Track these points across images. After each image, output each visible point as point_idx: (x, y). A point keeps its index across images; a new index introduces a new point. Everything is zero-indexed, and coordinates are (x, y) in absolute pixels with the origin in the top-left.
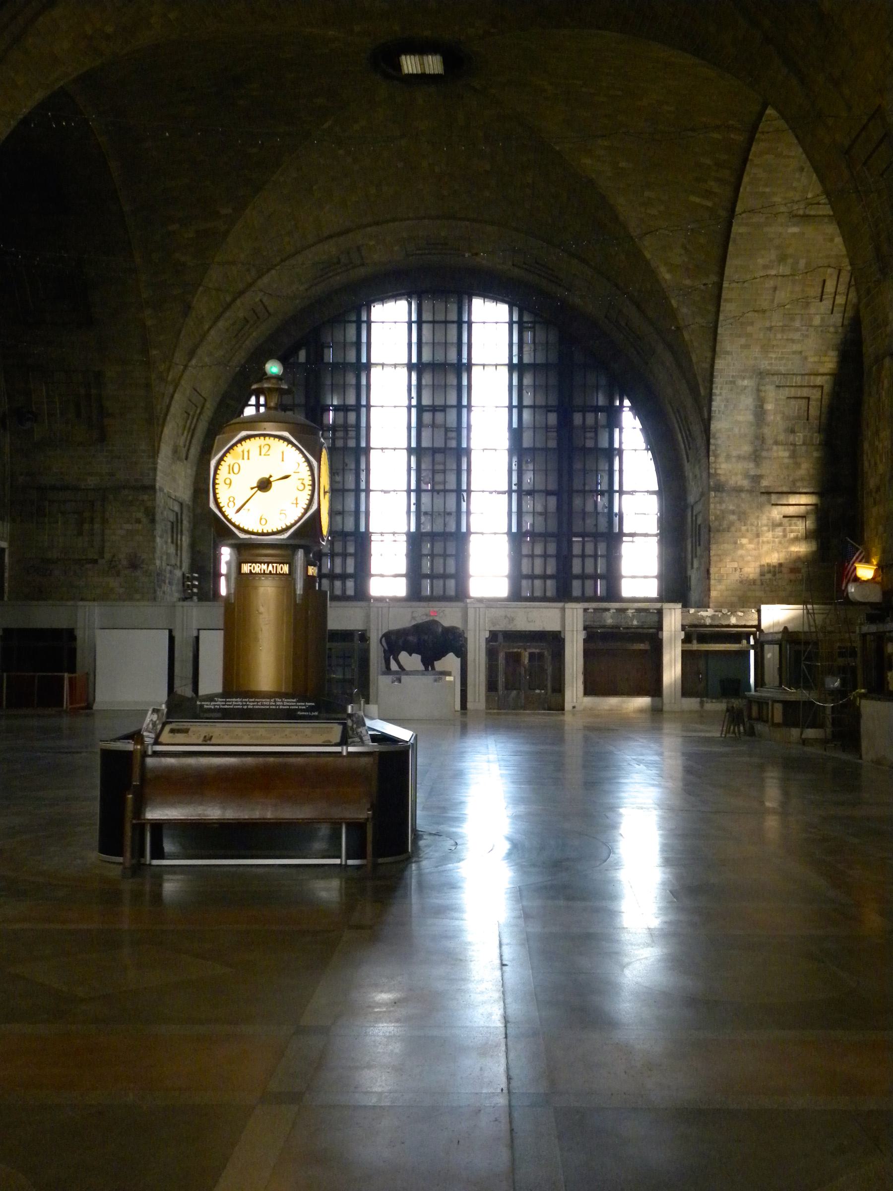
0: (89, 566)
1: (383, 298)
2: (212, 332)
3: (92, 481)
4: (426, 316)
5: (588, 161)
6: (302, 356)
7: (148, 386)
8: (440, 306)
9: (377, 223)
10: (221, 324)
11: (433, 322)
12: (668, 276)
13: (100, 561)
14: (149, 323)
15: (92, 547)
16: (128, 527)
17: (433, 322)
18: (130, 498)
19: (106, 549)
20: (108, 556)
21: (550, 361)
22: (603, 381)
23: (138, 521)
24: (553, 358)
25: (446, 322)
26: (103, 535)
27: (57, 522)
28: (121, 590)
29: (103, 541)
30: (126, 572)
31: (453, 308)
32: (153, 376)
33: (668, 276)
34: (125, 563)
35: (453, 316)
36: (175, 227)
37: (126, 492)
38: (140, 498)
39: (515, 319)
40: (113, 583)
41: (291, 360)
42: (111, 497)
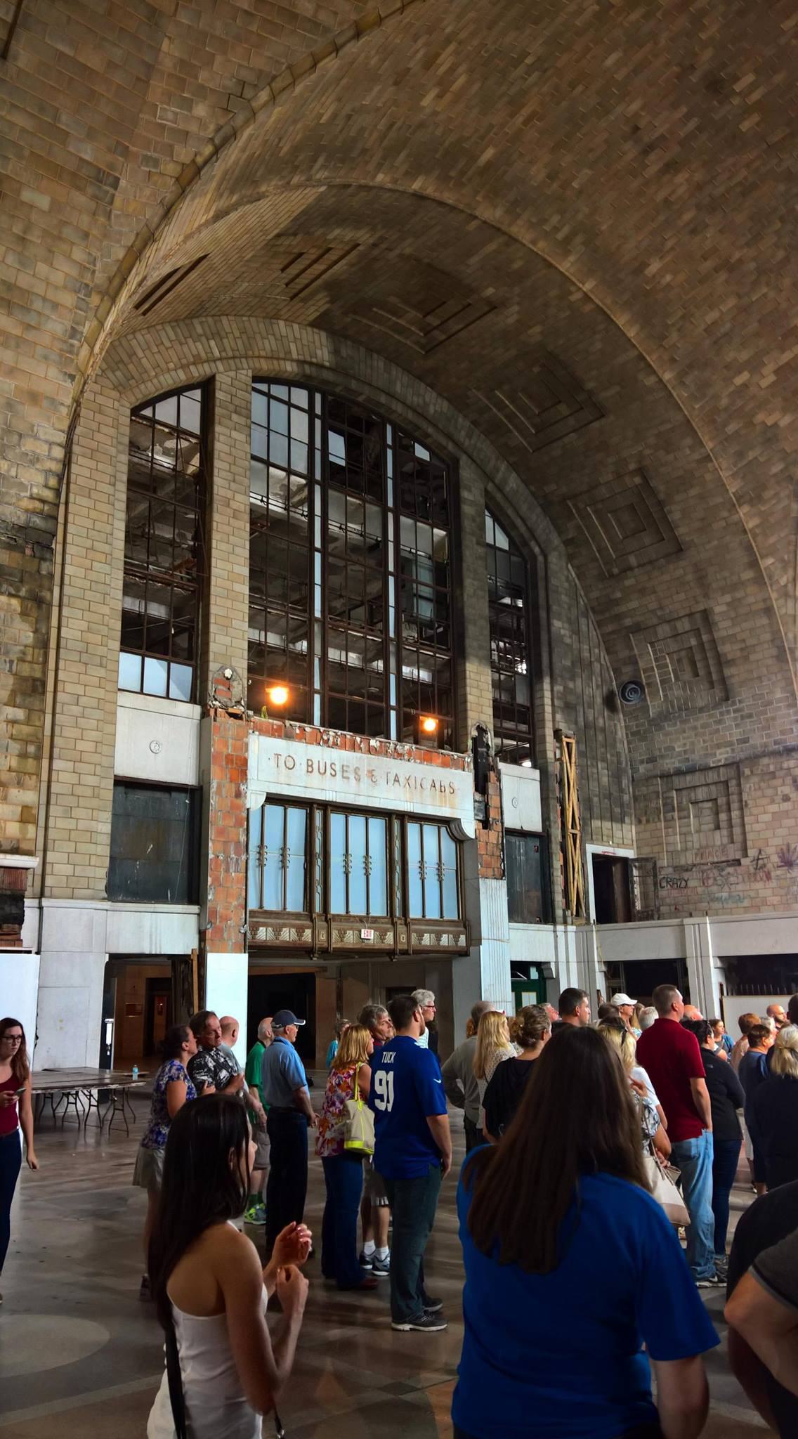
0: (731, 870)
3: (722, 756)
7: (769, 611)
13: (743, 861)
14: (750, 525)
15: (732, 842)
16: (773, 808)
18: (772, 768)
19: (749, 844)
20: (752, 853)
23: (786, 798)
26: (743, 825)
27: (689, 817)
28: (776, 900)
29: (744, 833)
30: (779, 872)
32: (774, 595)
34: (775, 859)
37: (765, 761)
38: (785, 765)
40: (763, 889)
42: (747, 772)
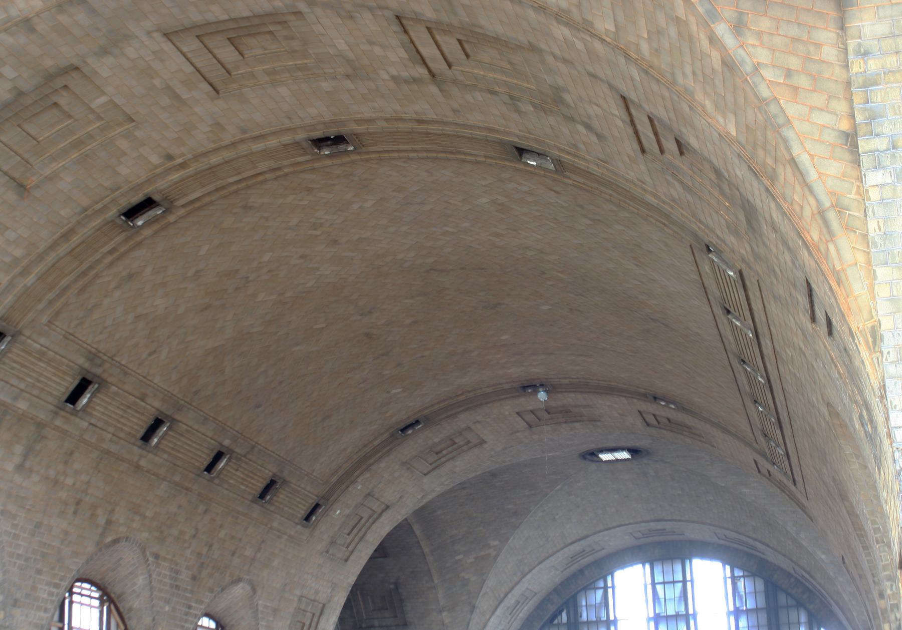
1: (623, 565)
2: (492, 619)
4: (659, 578)
5: (745, 490)
6: (564, 615)
8: (668, 567)
9: (607, 530)
10: (498, 612)
11: (664, 583)
12: (823, 557)
17: (664, 583)
21: (759, 606)
22: (803, 618)
24: (762, 603)
25: (674, 582)
31: (678, 567)
33: (823, 557)
35: (679, 577)
36: (461, 557)
39: (728, 574)
41: (556, 622)
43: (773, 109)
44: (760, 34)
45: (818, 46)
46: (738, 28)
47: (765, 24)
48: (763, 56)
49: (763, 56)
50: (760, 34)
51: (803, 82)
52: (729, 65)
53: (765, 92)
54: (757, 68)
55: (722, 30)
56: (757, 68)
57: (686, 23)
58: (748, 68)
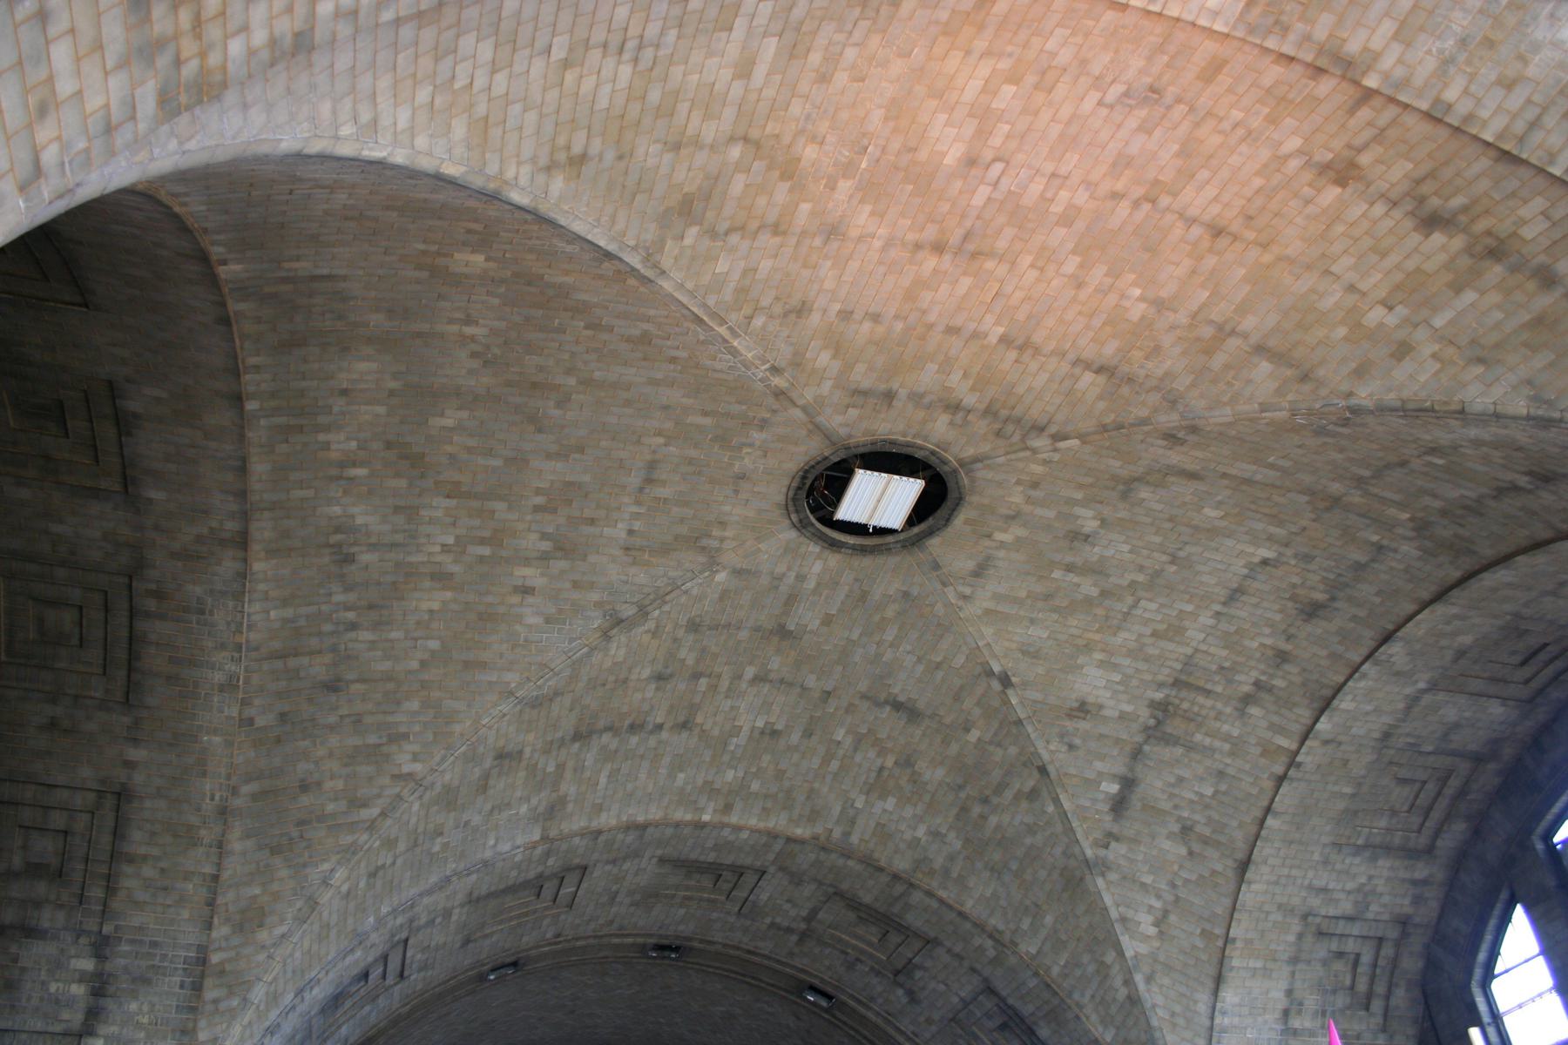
43: (1157, 1034)
44: (1161, 986)
45: (1196, 1002)
46: (1149, 979)
47: (1166, 981)
48: (1160, 1000)
49: (1160, 1000)
50: (1161, 986)
51: (1181, 1021)
52: (1134, 1000)
53: (1155, 1023)
54: (1154, 1006)
55: (1139, 978)
56: (1154, 1006)
57: (1109, 967)
58: (1148, 1005)
